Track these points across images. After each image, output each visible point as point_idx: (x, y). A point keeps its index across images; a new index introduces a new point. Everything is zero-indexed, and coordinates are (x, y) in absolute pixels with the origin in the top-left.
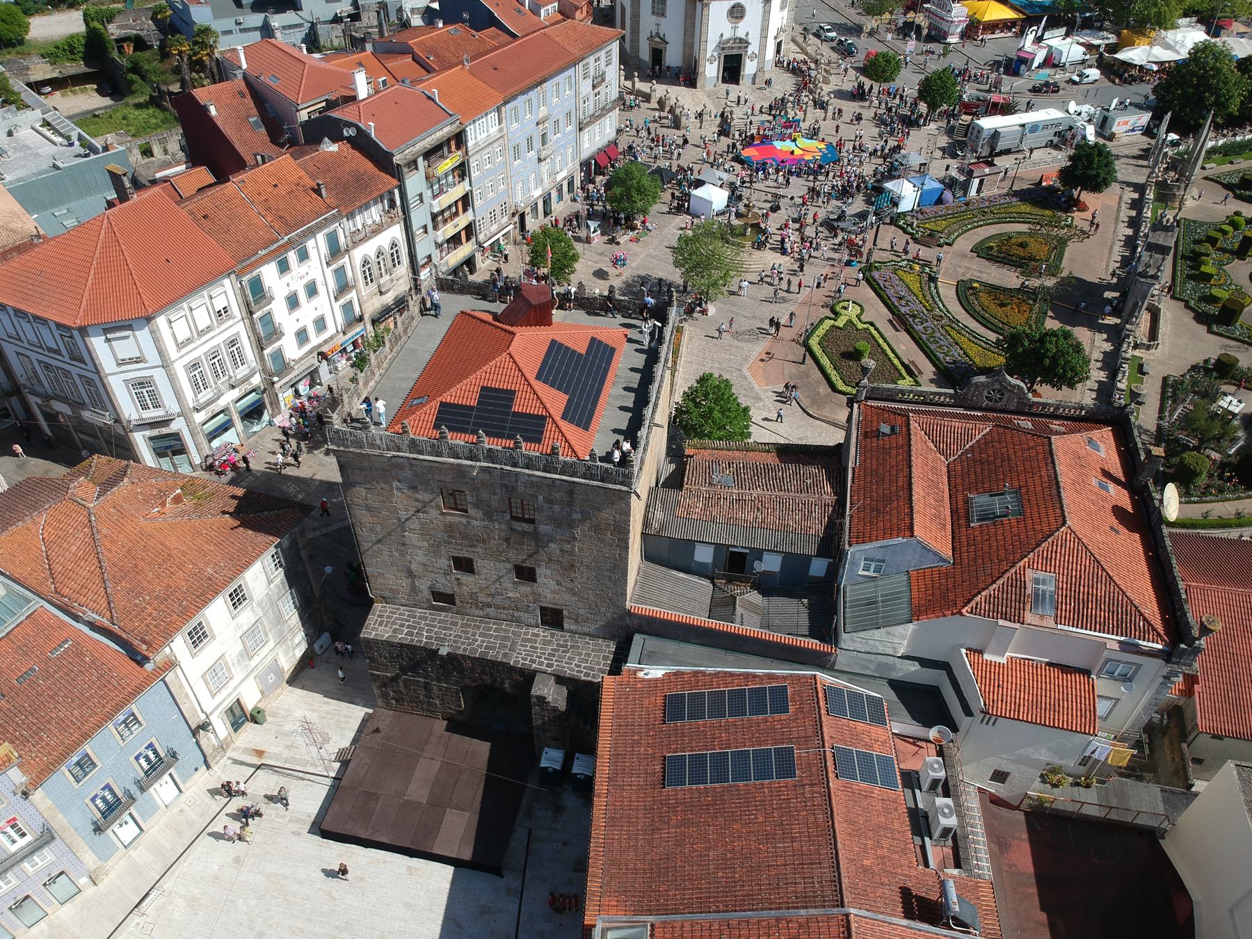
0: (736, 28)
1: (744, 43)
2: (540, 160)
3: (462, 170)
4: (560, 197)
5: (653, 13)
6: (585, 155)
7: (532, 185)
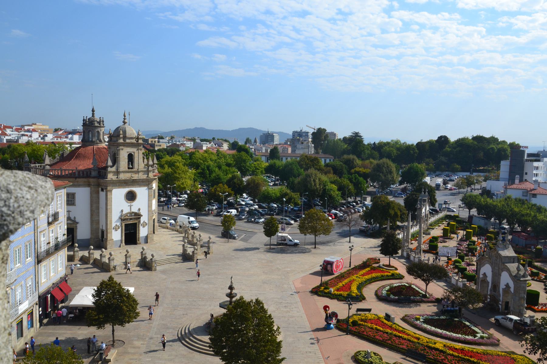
0: (131, 206)
1: (138, 216)
6: (43, 289)
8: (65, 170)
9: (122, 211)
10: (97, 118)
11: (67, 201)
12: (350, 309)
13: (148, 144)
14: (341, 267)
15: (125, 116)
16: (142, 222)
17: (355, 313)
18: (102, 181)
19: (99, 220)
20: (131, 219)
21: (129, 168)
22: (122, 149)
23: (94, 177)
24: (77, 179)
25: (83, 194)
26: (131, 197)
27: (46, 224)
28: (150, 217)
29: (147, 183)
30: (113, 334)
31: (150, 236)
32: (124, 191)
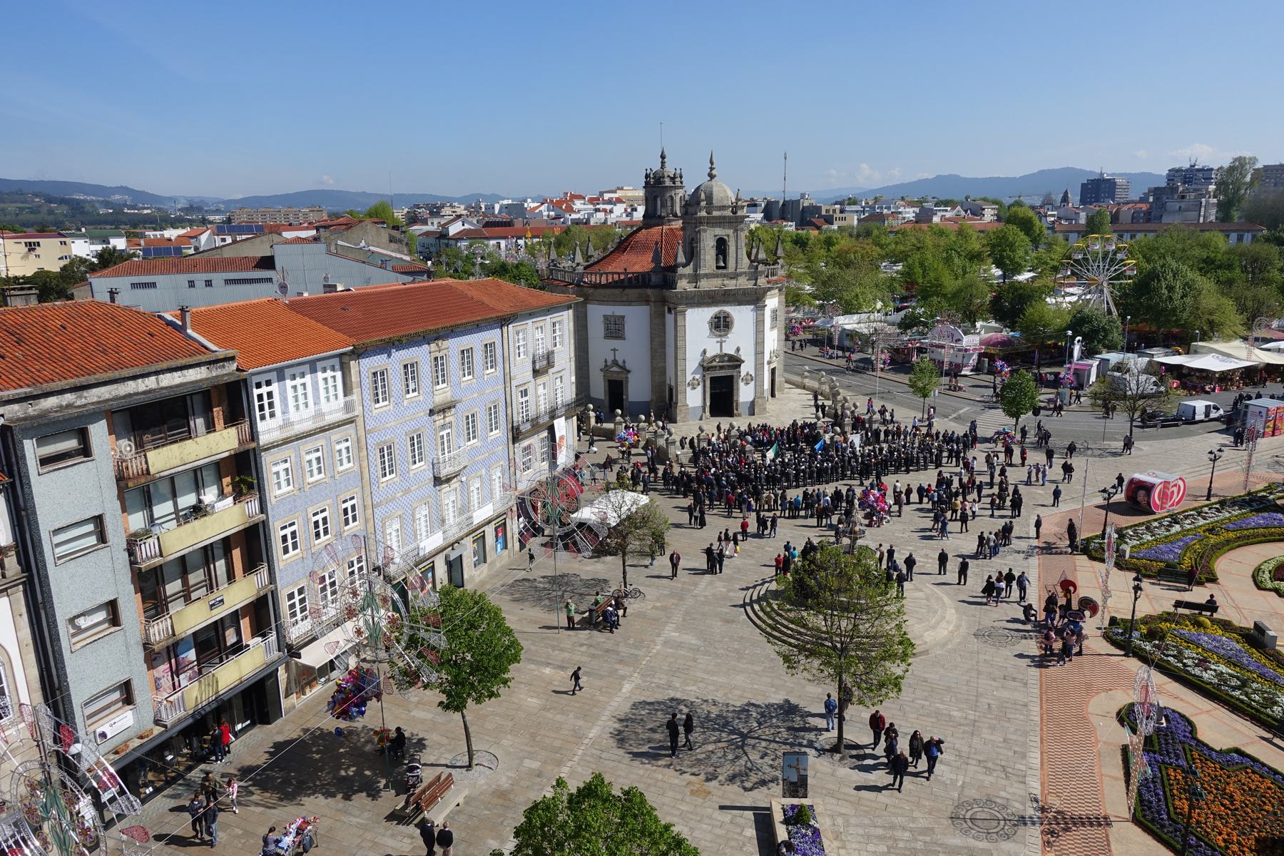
1: (735, 362)
2: (438, 481)
3: (242, 471)
4: (482, 557)
5: (607, 337)
7: (422, 526)
8: (613, 273)
9: (704, 352)
10: (670, 170)
11: (607, 329)
12: (1136, 599)
13: (821, 216)
14: (1176, 498)
15: (712, 163)
16: (743, 374)
17: (1172, 610)
18: (667, 293)
19: (664, 368)
20: (722, 368)
21: (718, 268)
22: (705, 231)
23: (654, 287)
24: (627, 291)
25: (636, 317)
26: (721, 325)
27: (530, 373)
28: (759, 366)
29: (755, 298)
30: (624, 578)
31: (759, 401)
32: (709, 312)
